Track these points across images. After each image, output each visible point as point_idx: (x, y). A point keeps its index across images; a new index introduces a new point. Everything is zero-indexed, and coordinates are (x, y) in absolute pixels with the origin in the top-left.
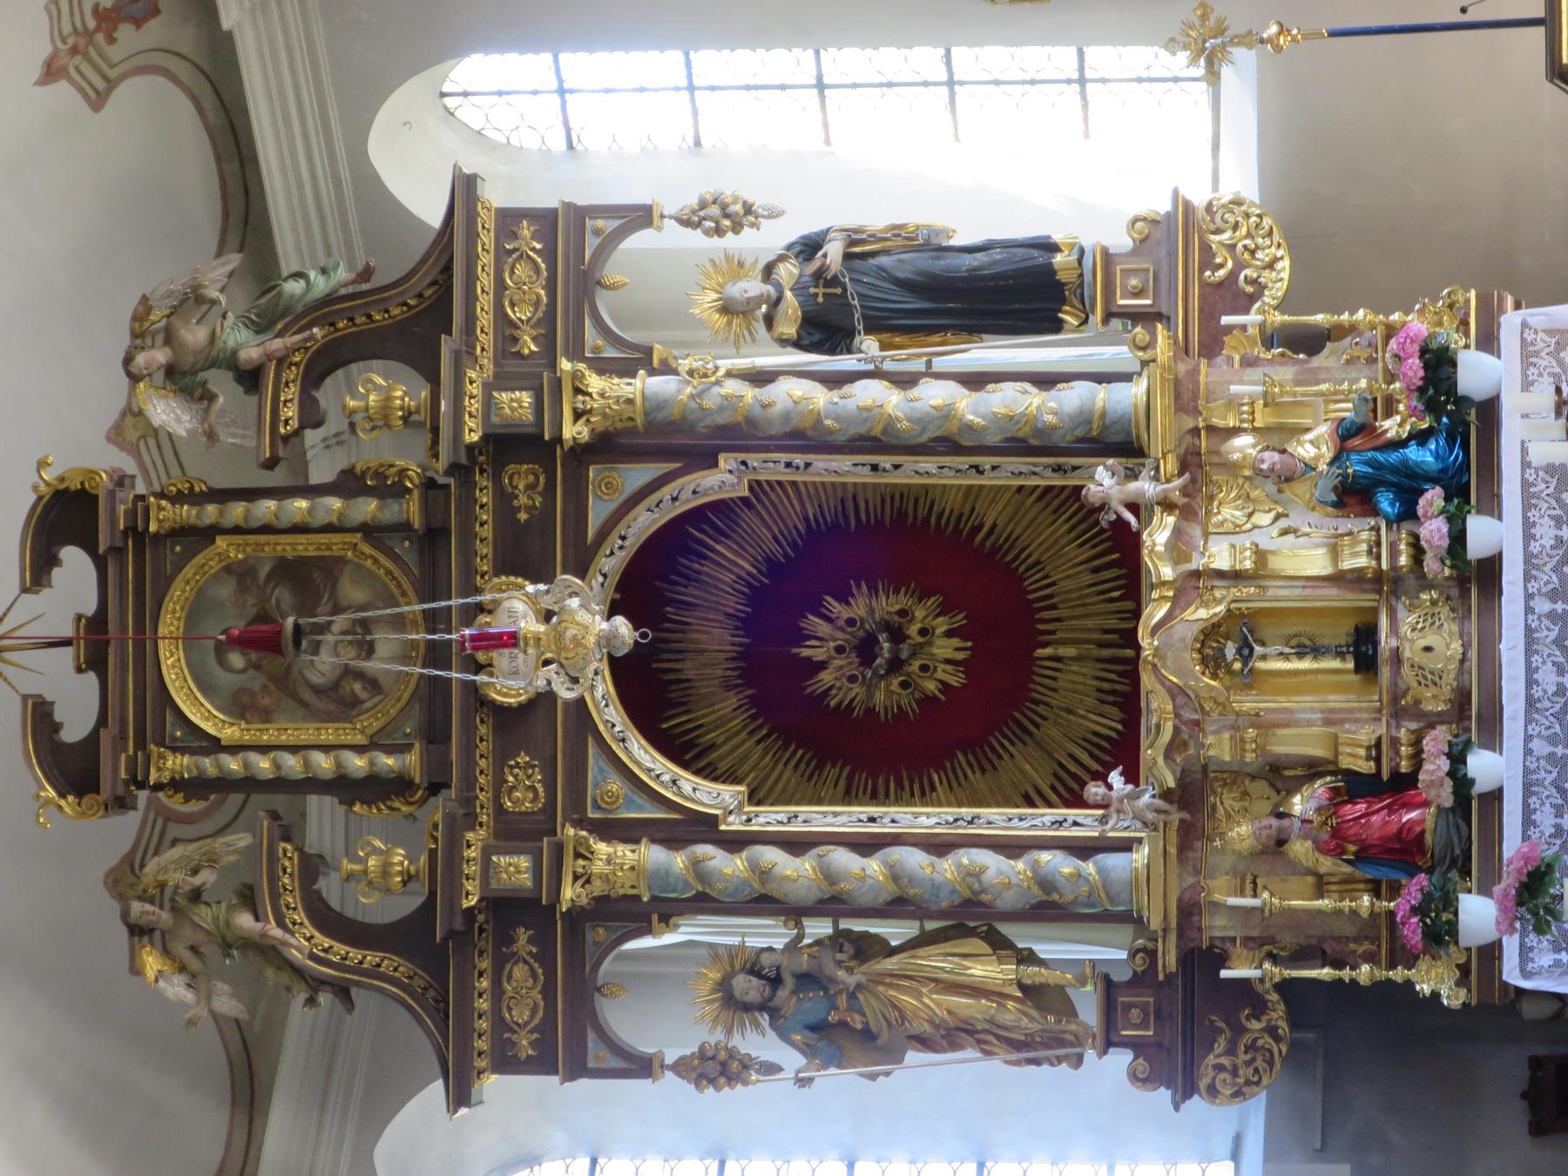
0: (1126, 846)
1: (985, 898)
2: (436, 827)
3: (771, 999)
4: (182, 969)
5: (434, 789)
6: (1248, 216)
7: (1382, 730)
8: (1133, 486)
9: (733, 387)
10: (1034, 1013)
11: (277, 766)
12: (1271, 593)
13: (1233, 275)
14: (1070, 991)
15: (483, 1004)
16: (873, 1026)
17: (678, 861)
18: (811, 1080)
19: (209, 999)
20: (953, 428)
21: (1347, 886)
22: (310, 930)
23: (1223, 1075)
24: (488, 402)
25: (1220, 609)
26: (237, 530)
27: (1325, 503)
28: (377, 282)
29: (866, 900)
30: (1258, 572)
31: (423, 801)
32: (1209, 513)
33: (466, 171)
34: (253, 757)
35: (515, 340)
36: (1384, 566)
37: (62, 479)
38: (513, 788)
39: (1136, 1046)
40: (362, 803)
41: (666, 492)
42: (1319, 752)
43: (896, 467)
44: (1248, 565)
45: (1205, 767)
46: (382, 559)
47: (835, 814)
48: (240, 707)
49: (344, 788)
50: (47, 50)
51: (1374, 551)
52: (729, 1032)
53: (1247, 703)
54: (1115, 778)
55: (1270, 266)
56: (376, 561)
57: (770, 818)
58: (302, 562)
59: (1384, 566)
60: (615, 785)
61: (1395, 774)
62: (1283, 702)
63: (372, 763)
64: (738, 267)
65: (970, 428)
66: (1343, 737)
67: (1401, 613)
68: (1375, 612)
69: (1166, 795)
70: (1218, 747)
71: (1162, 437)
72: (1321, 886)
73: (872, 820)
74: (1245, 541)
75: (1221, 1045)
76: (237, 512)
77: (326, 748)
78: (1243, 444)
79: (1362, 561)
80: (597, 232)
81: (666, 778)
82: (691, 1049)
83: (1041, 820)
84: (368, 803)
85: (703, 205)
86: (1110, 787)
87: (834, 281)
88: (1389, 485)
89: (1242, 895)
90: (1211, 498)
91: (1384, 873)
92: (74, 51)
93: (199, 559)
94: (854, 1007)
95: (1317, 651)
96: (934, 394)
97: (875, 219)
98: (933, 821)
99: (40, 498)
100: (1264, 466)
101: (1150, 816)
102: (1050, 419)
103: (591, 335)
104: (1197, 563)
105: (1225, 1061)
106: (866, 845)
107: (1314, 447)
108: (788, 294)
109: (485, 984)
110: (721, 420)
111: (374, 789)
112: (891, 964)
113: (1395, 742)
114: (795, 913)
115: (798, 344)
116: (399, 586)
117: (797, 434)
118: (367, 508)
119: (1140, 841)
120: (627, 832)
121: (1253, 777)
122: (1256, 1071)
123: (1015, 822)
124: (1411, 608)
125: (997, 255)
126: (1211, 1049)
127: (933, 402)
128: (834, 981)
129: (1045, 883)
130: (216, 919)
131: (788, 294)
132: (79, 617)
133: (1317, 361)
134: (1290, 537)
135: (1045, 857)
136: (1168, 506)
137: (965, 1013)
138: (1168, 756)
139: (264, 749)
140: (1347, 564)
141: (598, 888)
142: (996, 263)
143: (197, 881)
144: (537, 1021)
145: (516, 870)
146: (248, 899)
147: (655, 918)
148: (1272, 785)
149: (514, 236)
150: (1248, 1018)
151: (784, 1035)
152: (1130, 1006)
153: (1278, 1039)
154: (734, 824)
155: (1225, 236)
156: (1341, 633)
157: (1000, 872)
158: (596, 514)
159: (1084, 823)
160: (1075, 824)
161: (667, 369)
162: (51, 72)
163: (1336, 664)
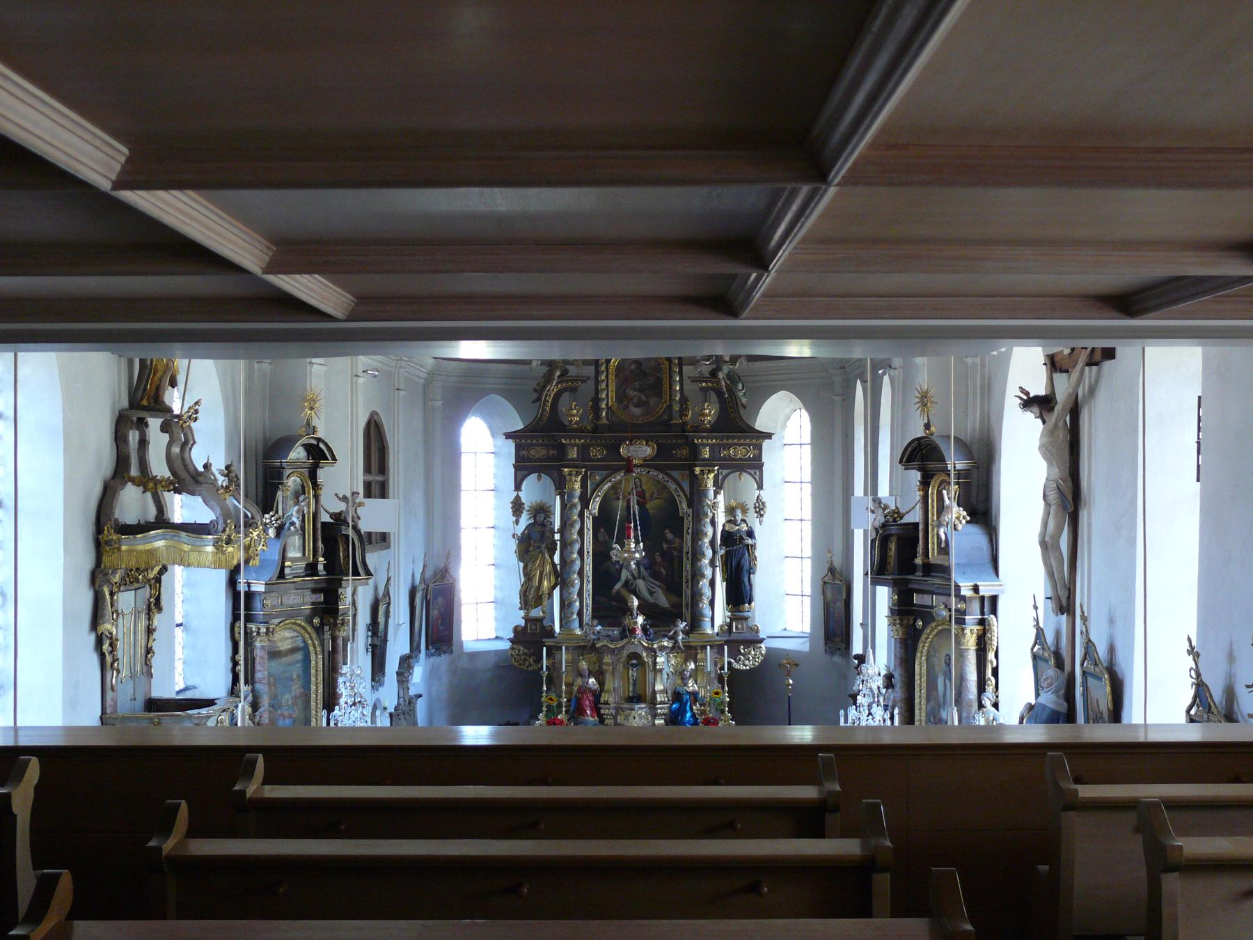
0: (581, 626)
1: (566, 587)
6: (758, 658)
9: (710, 515)
10: (534, 600)
11: (603, 381)
12: (650, 673)
14: (540, 607)
16: (530, 554)
17: (576, 500)
21: (569, 692)
23: (517, 652)
24: (707, 445)
25: (646, 660)
26: (670, 368)
28: (741, 409)
29: (565, 554)
30: (656, 671)
33: (773, 436)
34: (605, 374)
35: (724, 450)
39: (525, 628)
42: (606, 688)
44: (658, 667)
46: (662, 410)
47: (590, 542)
49: (596, 400)
52: (528, 511)
53: (620, 667)
55: (744, 665)
57: (589, 523)
59: (658, 706)
61: (600, 708)
63: (603, 409)
64: (745, 511)
65: (699, 583)
66: (610, 694)
67: (645, 710)
68: (645, 702)
70: (607, 659)
71: (694, 639)
73: (588, 552)
75: (525, 651)
77: (607, 395)
78: (692, 666)
79: (659, 699)
80: (755, 473)
81: (600, 494)
82: (523, 500)
83: (588, 600)
85: (763, 503)
86: (597, 626)
87: (740, 542)
88: (680, 707)
89: (566, 663)
90: (678, 653)
96: (708, 572)
98: (588, 569)
100: (685, 673)
101: (588, 638)
102: (701, 605)
103: (725, 472)
105: (521, 652)
106: (581, 553)
107: (692, 686)
108: (737, 528)
109: (540, 441)
110: (701, 512)
111: (596, 409)
112: (547, 556)
114: (561, 531)
115: (723, 531)
118: (676, 408)
119: (583, 630)
121: (599, 666)
122: (518, 661)
124: (646, 712)
125: (748, 588)
127: (705, 573)
128: (543, 543)
129: (570, 604)
131: (737, 528)
133: (716, 682)
134: (666, 676)
135: (577, 604)
139: (607, 377)
140: (658, 696)
141: (568, 478)
142: (745, 587)
144: (530, 456)
145: (573, 454)
149: (754, 449)
151: (527, 527)
152: (536, 625)
153: (527, 667)
155: (753, 652)
158: (676, 474)
161: (716, 493)
163: (631, 689)
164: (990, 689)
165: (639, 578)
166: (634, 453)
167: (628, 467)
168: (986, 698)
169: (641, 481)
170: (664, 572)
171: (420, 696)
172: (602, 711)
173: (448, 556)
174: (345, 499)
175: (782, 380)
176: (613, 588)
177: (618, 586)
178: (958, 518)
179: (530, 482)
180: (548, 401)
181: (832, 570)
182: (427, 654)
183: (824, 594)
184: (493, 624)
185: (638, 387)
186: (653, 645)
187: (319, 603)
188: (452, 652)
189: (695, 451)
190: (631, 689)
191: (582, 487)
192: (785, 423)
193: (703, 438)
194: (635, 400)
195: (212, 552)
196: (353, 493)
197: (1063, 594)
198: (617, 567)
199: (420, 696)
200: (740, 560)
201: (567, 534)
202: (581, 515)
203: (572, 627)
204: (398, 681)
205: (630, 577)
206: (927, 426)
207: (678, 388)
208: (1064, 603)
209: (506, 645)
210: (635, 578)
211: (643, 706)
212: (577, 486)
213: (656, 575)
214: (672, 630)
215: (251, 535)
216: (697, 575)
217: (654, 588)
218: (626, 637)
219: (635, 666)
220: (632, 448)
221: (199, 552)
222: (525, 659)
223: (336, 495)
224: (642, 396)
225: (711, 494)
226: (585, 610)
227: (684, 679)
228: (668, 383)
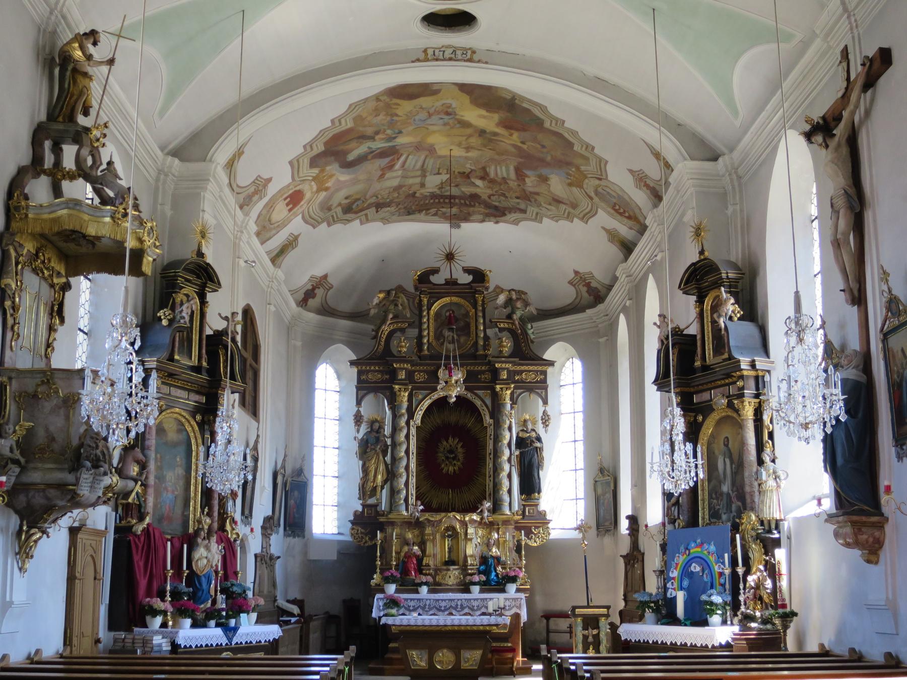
0: (407, 509)
4: (380, 302)
5: (420, 357)
7: (432, 567)
9: (508, 422)
13: (533, 533)
15: (372, 368)
17: (404, 411)
20: (499, 471)
21: (398, 559)
22: (389, 330)
24: (504, 369)
28: (531, 344)
30: (467, 539)
34: (426, 318)
41: (485, 408)
48: (438, 314)
49: (420, 337)
50: (581, 272)
53: (438, 536)
54: (422, 507)
55: (535, 541)
57: (413, 431)
58: (469, 328)
60: (420, 397)
61: (423, 570)
62: (438, 545)
64: (534, 423)
65: (499, 475)
67: (458, 571)
68: (458, 565)
69: (418, 519)
70: (428, 530)
71: (498, 517)
72: (398, 553)
74: (474, 536)
75: (363, 531)
76: (480, 314)
77: (428, 334)
78: (496, 536)
79: (469, 562)
82: (362, 413)
83: (413, 491)
84: (417, 342)
85: (548, 416)
88: (486, 569)
91: (400, 567)
92: (581, 278)
94: (372, 449)
95: (450, 552)
96: (506, 467)
97: (545, 454)
103: (519, 391)
104: (469, 526)
106: (407, 452)
107: (495, 551)
111: (420, 344)
112: (381, 457)
115: (517, 437)
117: (498, 437)
118: (481, 343)
121: (422, 538)
125: (537, 481)
129: (399, 492)
133: (514, 552)
135: (405, 492)
136: (482, 519)
139: (428, 320)
140: (469, 559)
141: (398, 393)
145: (402, 375)
146: (395, 317)
149: (541, 374)
151: (365, 434)
153: (364, 543)
154: (412, 423)
156: (454, 557)
158: (480, 392)
159: (412, 500)
161: (512, 408)
162: (576, 273)
164: (768, 450)
168: (766, 455)
171: (279, 557)
173: (303, 459)
174: (226, 319)
175: (560, 334)
178: (733, 312)
179: (369, 400)
181: (602, 470)
182: (285, 535)
183: (595, 490)
184: (336, 523)
188: (304, 537)
189: (495, 373)
191: (408, 401)
192: (561, 369)
193: (503, 362)
196: (233, 314)
197: (854, 286)
199: (279, 557)
200: (531, 458)
201: (397, 437)
204: (262, 534)
206: (702, 252)
208: (856, 293)
209: (348, 538)
211: (456, 567)
212: (406, 399)
216: (497, 469)
221: (99, 222)
223: (220, 315)
225: (508, 407)
227: (488, 546)
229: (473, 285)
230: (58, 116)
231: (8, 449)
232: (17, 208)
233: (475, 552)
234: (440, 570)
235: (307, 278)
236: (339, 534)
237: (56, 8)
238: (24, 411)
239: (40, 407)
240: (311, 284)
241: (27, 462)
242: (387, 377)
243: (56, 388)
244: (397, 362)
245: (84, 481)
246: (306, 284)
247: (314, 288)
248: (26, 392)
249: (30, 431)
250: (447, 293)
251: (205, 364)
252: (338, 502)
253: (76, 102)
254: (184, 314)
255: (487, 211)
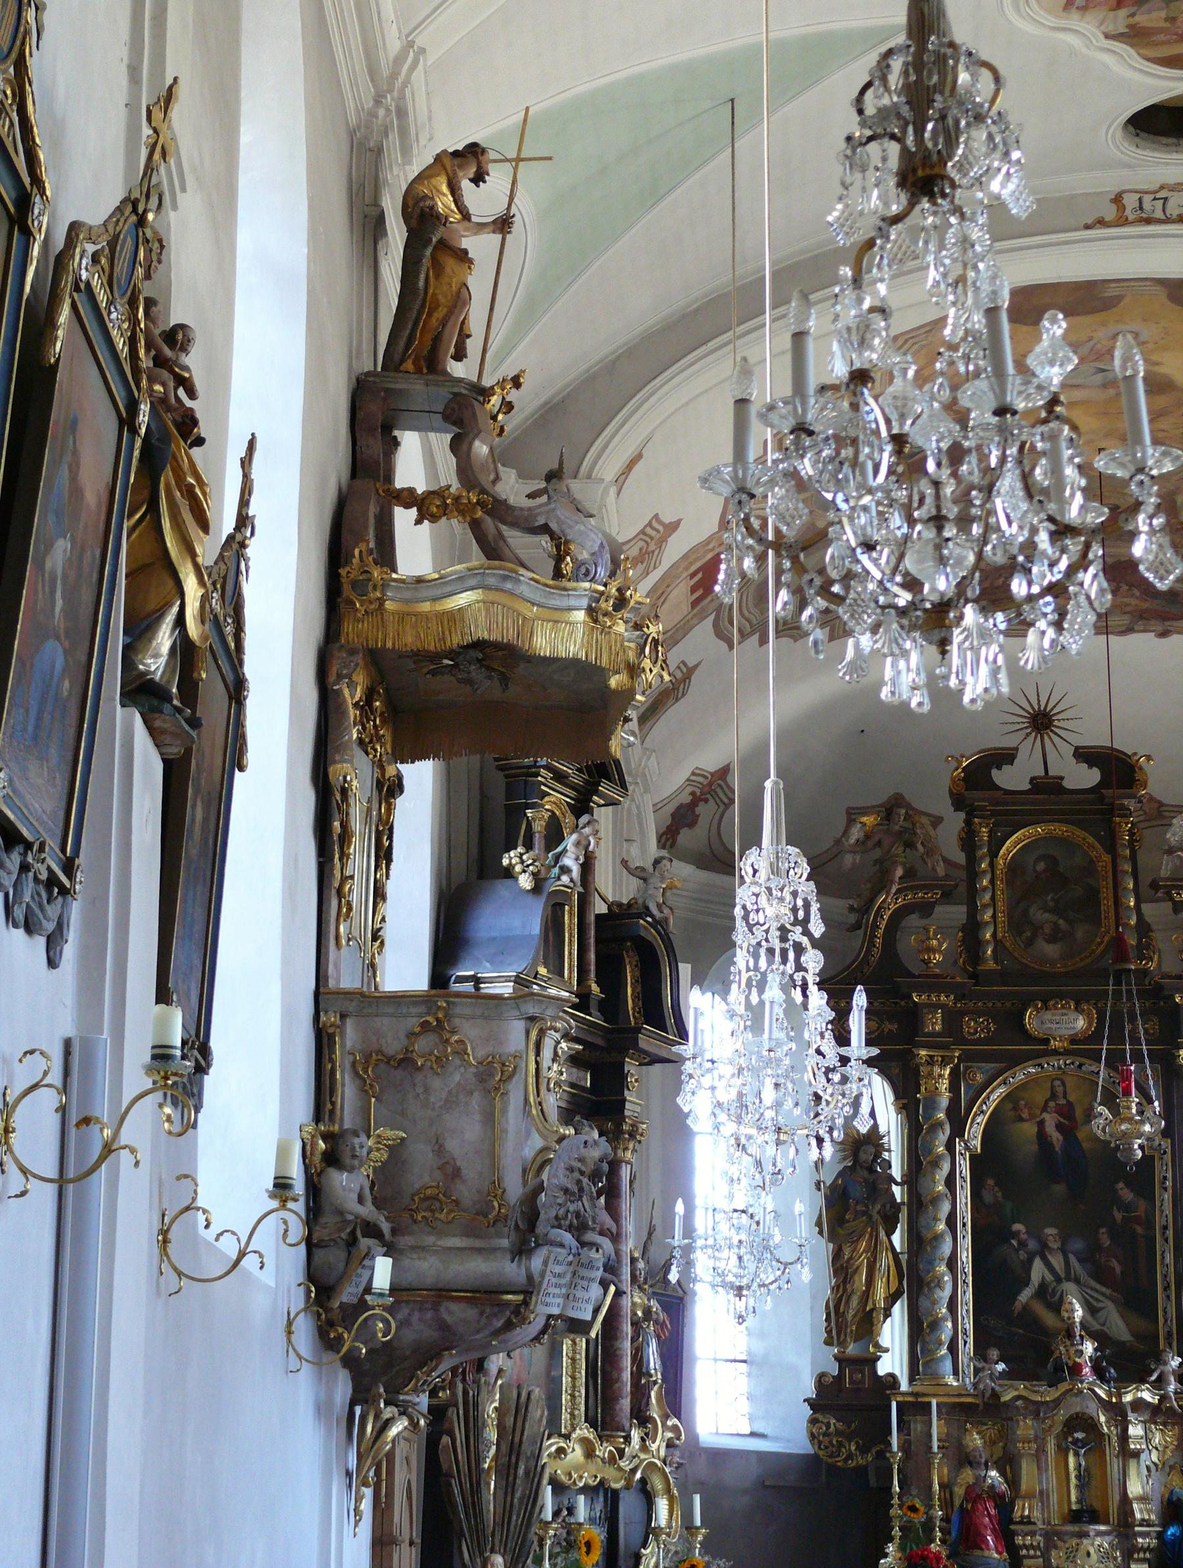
0: (956, 1373)
2: (953, 978)
3: (861, 1167)
4: (867, 837)
5: (973, 976)
8: (1172, 1379)
10: (857, 1319)
17: (941, 1115)
18: (819, 1189)
19: (851, 852)
21: (947, 1504)
27: (1171, 1493)
29: (922, 1221)
30: (1128, 1455)
31: (965, 970)
32: (1155, 1423)
34: (989, 876)
36: (1137, 1529)
37: (1141, 768)
38: (976, 1022)
39: (840, 1378)
40: (964, 937)
42: (1024, 1487)
43: (1166, 1240)
45: (1012, 1419)
48: (1015, 867)
49: (972, 928)
51: (1145, 1523)
53: (1051, 1446)
54: (1001, 1367)
56: (1100, 944)
57: (964, 1167)
58: (1098, 903)
59: (1137, 1529)
60: (980, 1078)
63: (988, 942)
66: (1034, 1501)
67: (1108, 1538)
68: (1106, 1522)
70: (1026, 1427)
75: (840, 1425)
76: (1128, 867)
77: (994, 916)
79: (1138, 1516)
81: (984, 1107)
84: (963, 941)
89: (939, 1440)
93: (1097, 844)
94: (857, 1214)
95: (1081, 1487)
98: (964, 1260)
99: (1129, 757)
101: (981, 1386)
104: (1131, 1417)
106: (951, 1221)
113: (1033, 1534)
116: (1086, 957)
120: (954, 1088)
121: (1004, 1447)
122: (826, 1447)
123: (965, 1307)
126: (838, 1420)
128: (873, 1205)
129: (935, 1325)
130: (897, 855)
132: (1062, 778)
134: (1145, 1472)
135: (949, 1324)
136: (1164, 1398)
137: (856, 1278)
138: (1018, 1397)
139: (992, 882)
140: (1135, 1506)
141: (924, 1070)
143: (919, 846)
145: (935, 1023)
146: (909, 874)
147: (905, 1101)
148: (1000, 1458)
150: (857, 1443)
151: (840, 1174)
152: (863, 1375)
153: (846, 1460)
154: (959, 1147)
157: (941, 1298)
160: (965, 1343)
163: (1073, 1498)
165: (1068, 1279)
166: (1054, 1026)
167: (1040, 1047)
169: (1064, 1084)
170: (1118, 1269)
172: (1019, 1540)
176: (1014, 1299)
177: (1025, 1296)
180: (878, 927)
184: (745, 1406)
185: (1051, 904)
186: (1119, 1396)
187: (583, 1089)
190: (1073, 1498)
194: (1047, 930)
195: (584, 622)
198: (1023, 1255)
201: (924, 1182)
202: (950, 1146)
203: (941, 1372)
205: (1049, 1277)
207: (1132, 904)
210: (1059, 1280)
211: (1103, 1528)
212: (944, 1085)
213: (1101, 1274)
214: (1154, 1371)
215: (645, 629)
217: (1098, 1300)
218: (1065, 1380)
219: (1083, 1443)
220: (1048, 1015)
222: (840, 1444)
224: (1061, 922)
226: (961, 1343)
228: (1111, 895)
229: (1107, 792)
230: (402, 361)
231: (355, 1197)
232: (360, 587)
233: (1148, 1489)
234: (1060, 1535)
235: (686, 774)
236: (753, 1434)
237: (391, 91)
238: (377, 1099)
239: (420, 1090)
240: (689, 789)
241: (394, 1231)
242: (894, 1027)
243: (461, 1042)
244: (921, 990)
245: (554, 1280)
246: (680, 790)
247: (696, 800)
248: (380, 1052)
249: (396, 1150)
250: (1047, 812)
251: (595, 988)
252: (749, 1353)
253: (444, 323)
254: (568, 861)
255: (1146, 605)
